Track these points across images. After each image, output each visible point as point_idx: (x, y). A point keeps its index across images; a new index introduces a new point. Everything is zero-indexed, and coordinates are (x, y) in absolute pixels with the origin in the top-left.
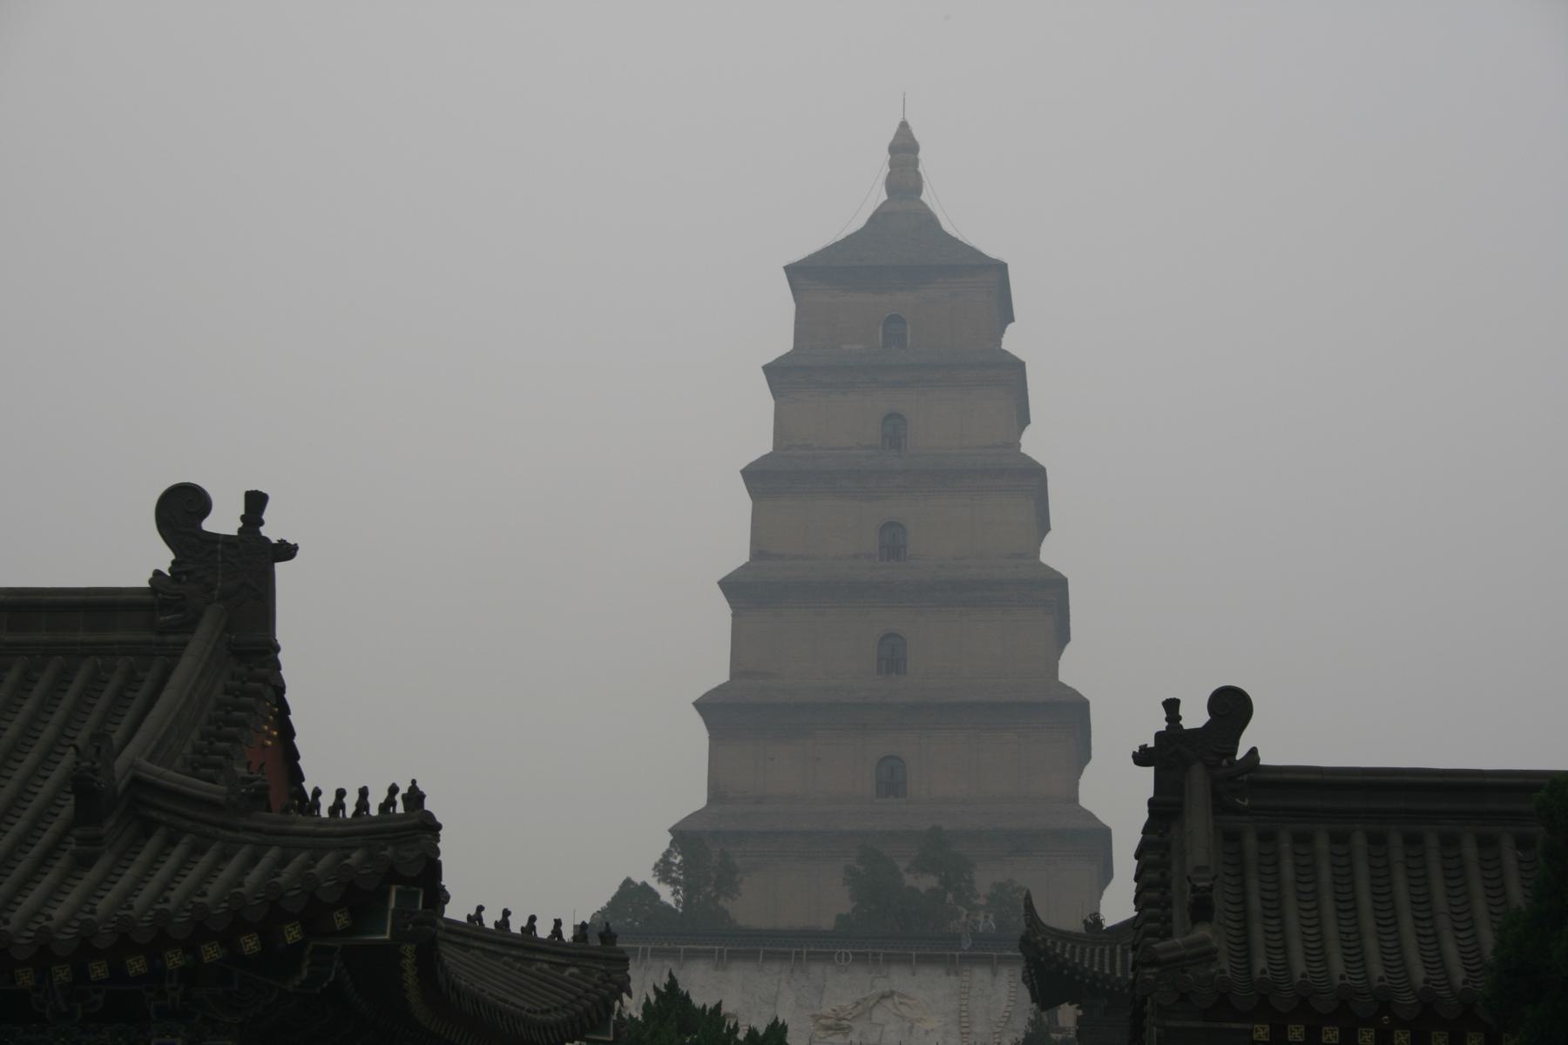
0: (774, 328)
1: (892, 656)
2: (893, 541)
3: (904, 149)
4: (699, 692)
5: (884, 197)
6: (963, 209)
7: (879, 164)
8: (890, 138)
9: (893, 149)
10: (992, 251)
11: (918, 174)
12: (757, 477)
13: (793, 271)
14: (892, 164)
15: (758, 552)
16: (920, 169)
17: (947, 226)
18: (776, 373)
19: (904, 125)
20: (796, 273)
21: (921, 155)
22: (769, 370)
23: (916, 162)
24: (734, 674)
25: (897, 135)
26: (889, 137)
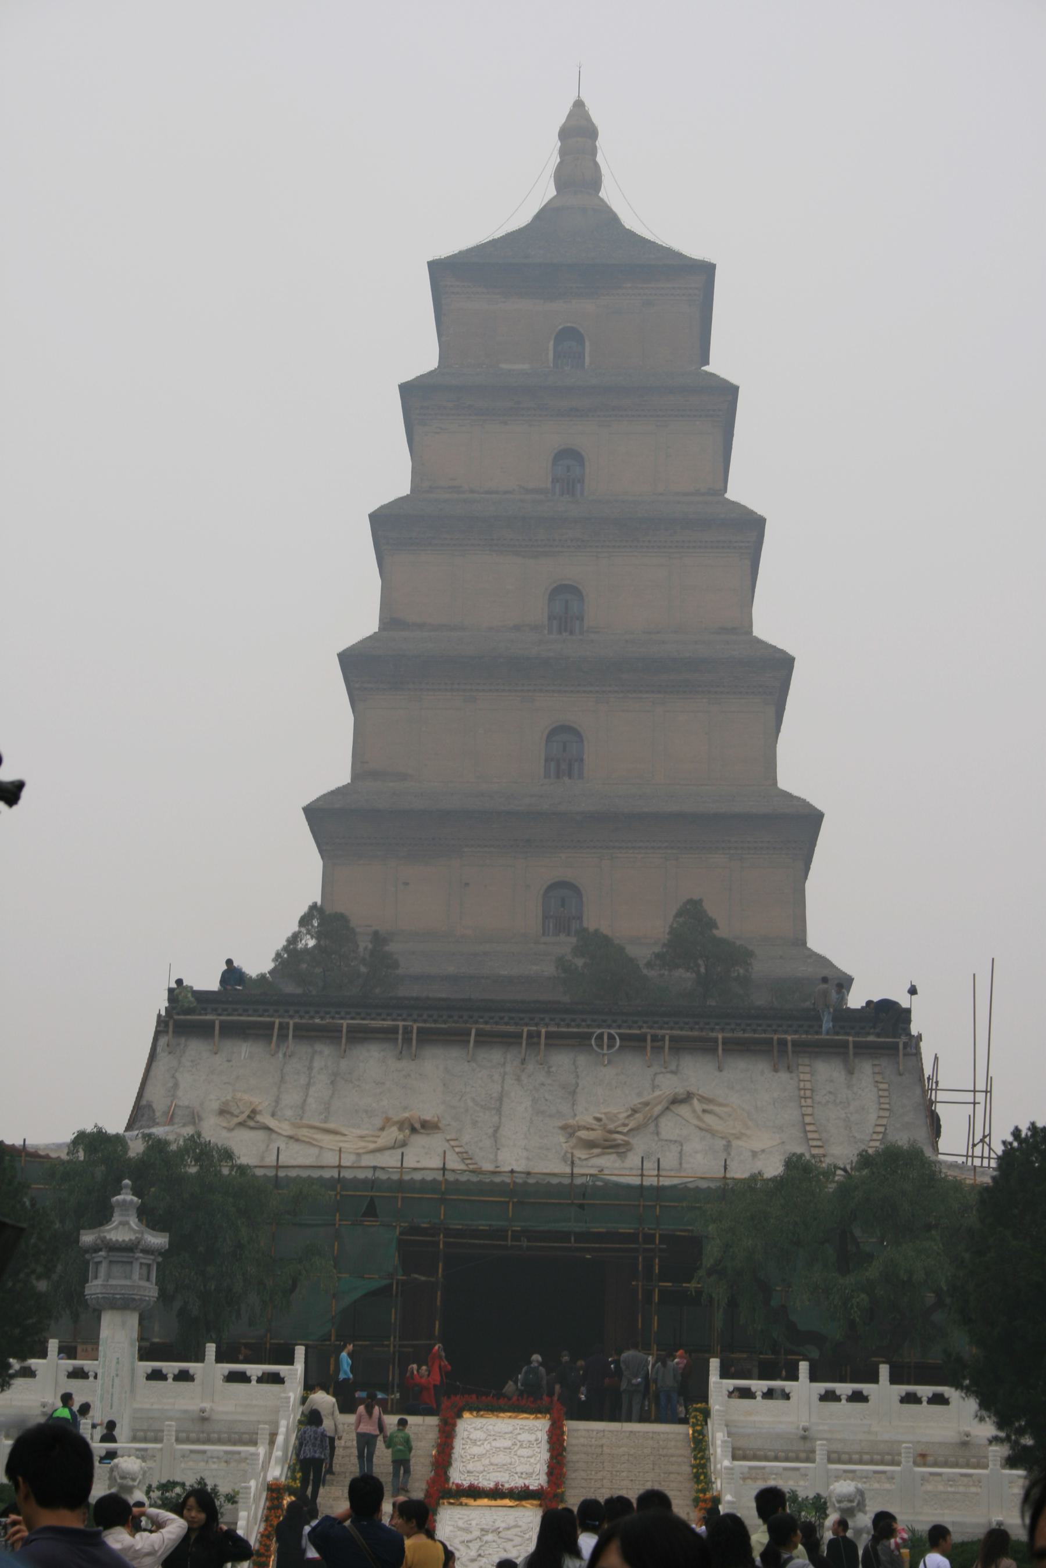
1: (564, 751)
2: (566, 603)
3: (579, 135)
4: (310, 796)
5: (552, 192)
7: (548, 153)
8: (561, 120)
9: (565, 134)
10: (694, 249)
11: (596, 166)
12: (391, 528)
13: (437, 268)
14: (563, 153)
15: (389, 620)
16: (599, 159)
17: (630, 221)
18: (416, 396)
19: (579, 104)
21: (600, 142)
22: (406, 389)
23: (594, 151)
24: (355, 776)
25: (570, 116)
26: (560, 118)
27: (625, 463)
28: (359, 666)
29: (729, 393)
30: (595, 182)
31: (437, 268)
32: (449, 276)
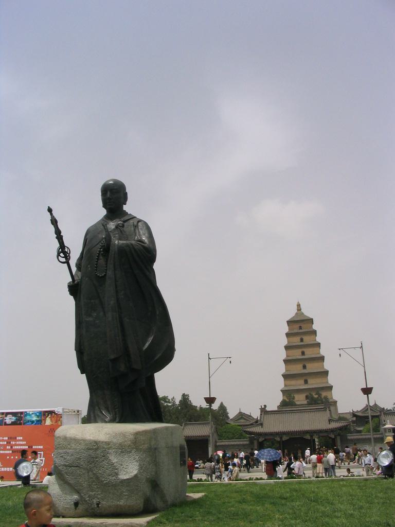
0: (286, 329)
1: (304, 367)
3: (299, 305)
6: (308, 312)
10: (311, 317)
13: (288, 322)
15: (287, 356)
20: (288, 322)
22: (286, 334)
24: (286, 371)
27: (308, 340)
28: (285, 361)
29: (316, 331)
30: (300, 310)
31: (288, 322)
32: (289, 322)
